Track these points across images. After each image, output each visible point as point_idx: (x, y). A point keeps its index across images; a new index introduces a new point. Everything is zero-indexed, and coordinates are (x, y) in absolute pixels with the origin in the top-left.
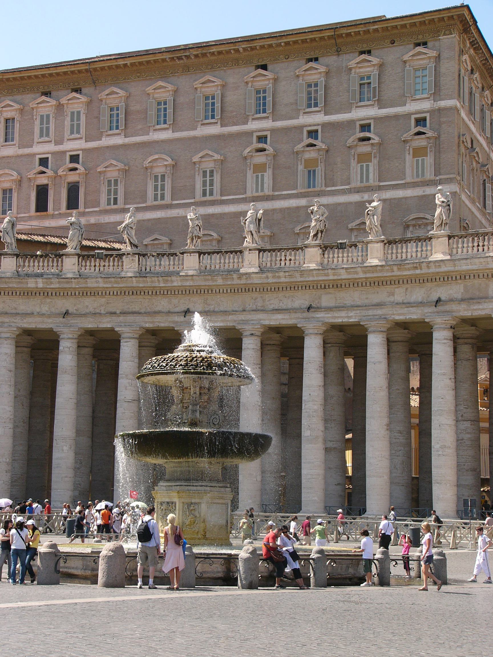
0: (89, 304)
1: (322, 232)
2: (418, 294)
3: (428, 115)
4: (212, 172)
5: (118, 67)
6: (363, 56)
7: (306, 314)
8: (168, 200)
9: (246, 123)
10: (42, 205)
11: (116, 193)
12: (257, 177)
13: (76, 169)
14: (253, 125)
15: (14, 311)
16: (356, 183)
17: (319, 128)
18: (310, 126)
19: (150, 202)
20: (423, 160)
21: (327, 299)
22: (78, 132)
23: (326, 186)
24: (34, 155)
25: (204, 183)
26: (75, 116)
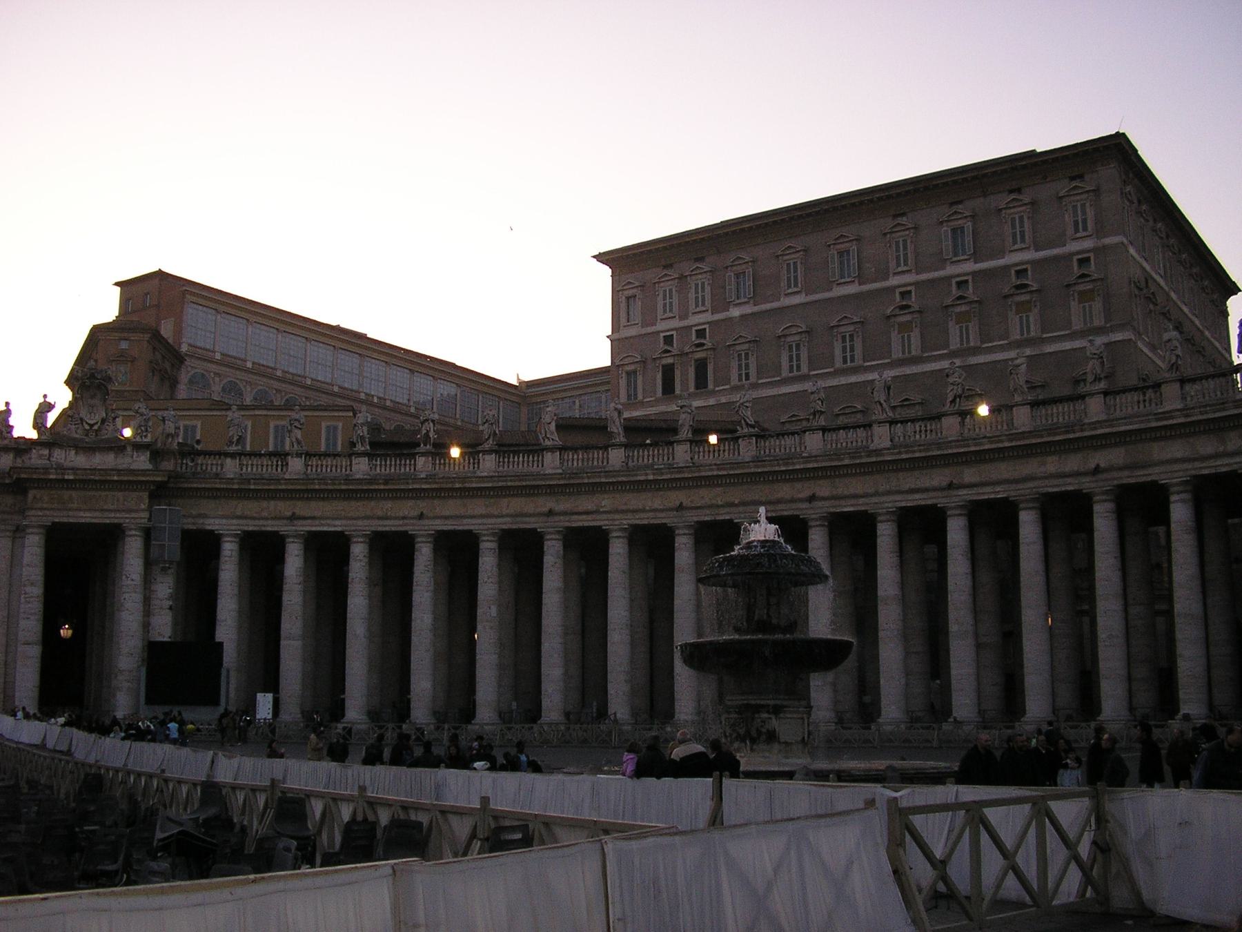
0: (705, 496)
1: (960, 397)
2: (1073, 463)
3: (1092, 255)
4: (852, 336)
5: (743, 230)
6: (1013, 196)
7: (945, 493)
8: (805, 369)
9: (887, 279)
10: (668, 388)
11: (747, 366)
12: (903, 337)
13: (703, 345)
14: (894, 281)
15: (624, 508)
16: (1015, 336)
17: (970, 278)
18: (958, 276)
19: (785, 373)
20: (1090, 307)
21: (970, 475)
22: (703, 304)
23: (983, 342)
24: (658, 332)
25: (844, 349)
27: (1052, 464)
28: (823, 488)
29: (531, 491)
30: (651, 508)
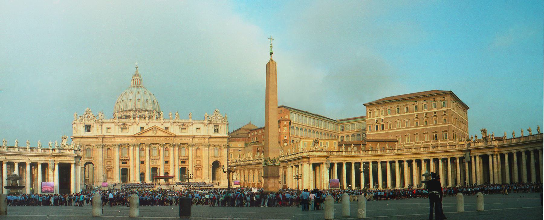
0: (399, 157)
2: (446, 154)
10: (377, 129)
21: (433, 155)
26: (382, 111)
27: (443, 154)
28: (415, 156)
29: (376, 156)
30: (392, 158)
